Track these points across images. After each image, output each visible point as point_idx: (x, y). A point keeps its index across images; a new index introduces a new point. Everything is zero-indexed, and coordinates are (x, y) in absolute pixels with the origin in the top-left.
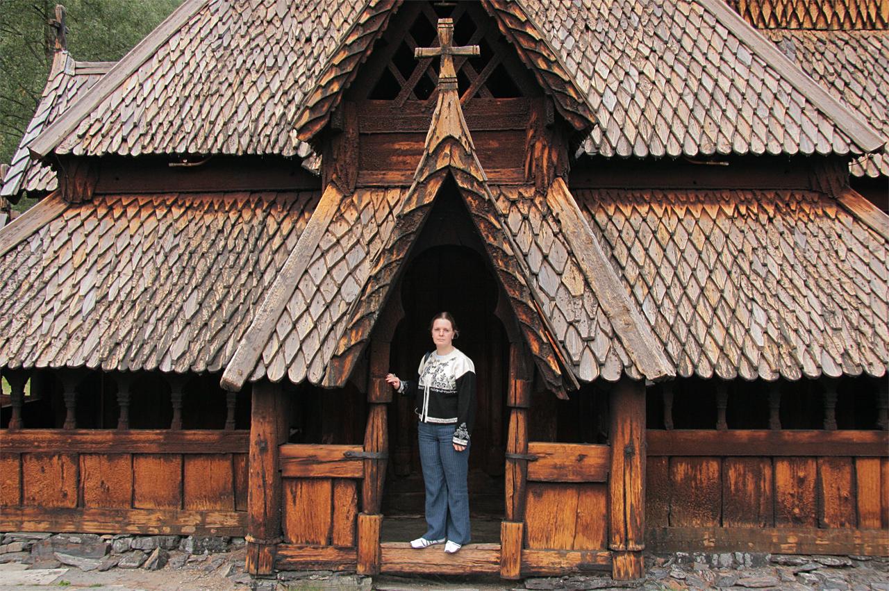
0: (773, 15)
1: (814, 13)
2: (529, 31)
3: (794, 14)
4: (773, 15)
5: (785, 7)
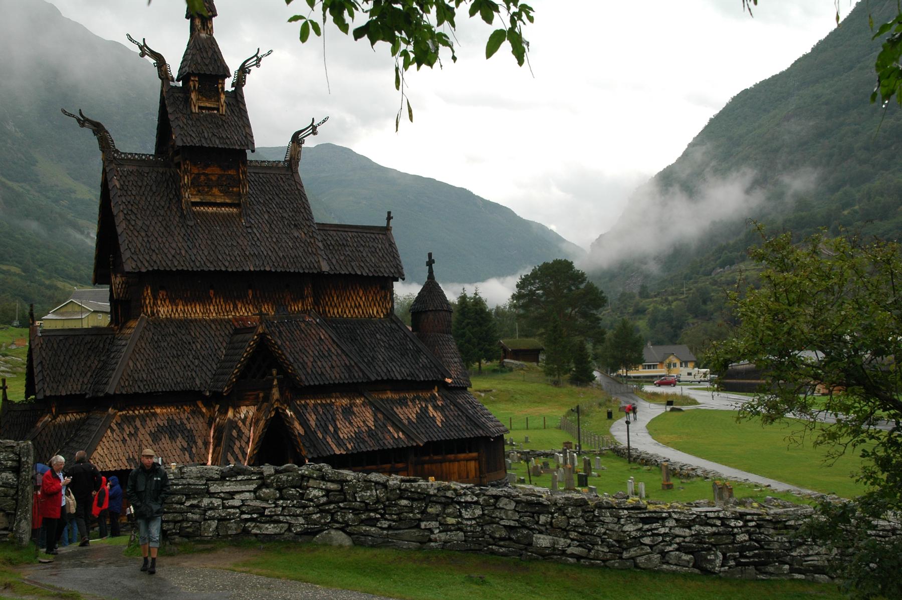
0: (338, 312)
1: (352, 312)
2: (286, 361)
3: (345, 312)
4: (338, 312)
5: (342, 309)
